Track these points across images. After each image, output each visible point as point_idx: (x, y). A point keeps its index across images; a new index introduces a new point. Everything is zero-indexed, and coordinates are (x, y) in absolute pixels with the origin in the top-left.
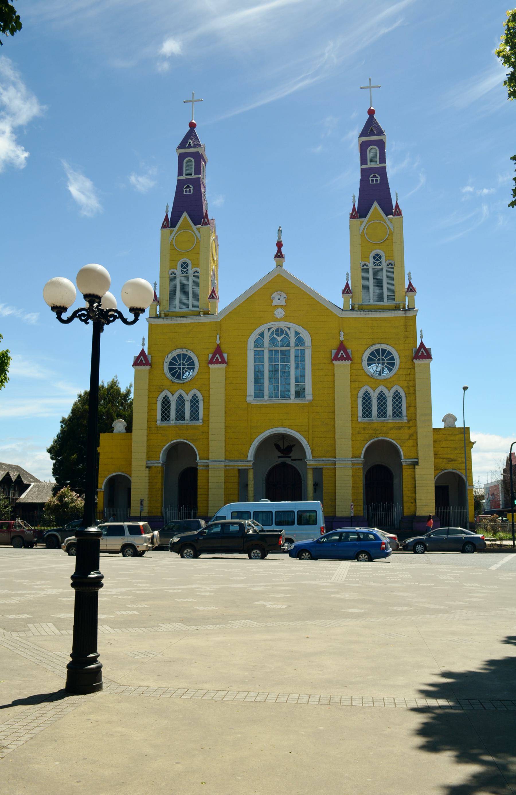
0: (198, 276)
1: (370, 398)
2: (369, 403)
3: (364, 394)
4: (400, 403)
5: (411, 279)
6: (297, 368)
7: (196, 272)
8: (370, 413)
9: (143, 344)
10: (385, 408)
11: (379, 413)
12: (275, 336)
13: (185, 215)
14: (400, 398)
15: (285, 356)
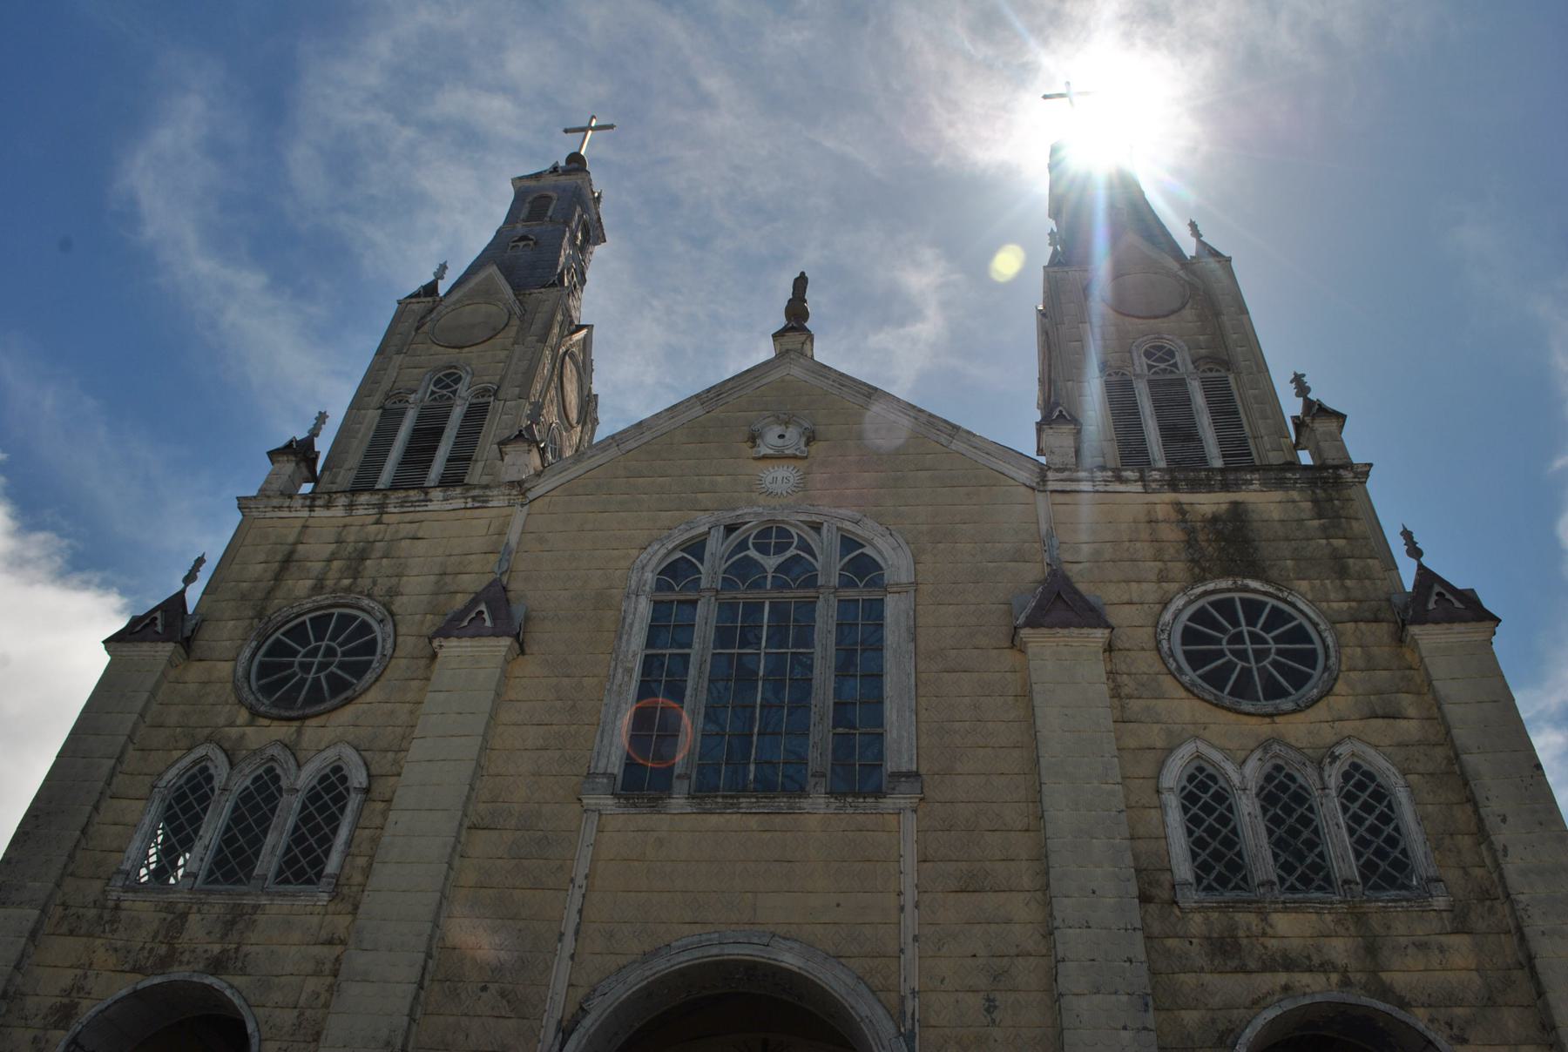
1: (1220, 797)
2: (1224, 820)
3: (1191, 778)
4: (1386, 819)
5: (1308, 390)
6: (844, 669)
8: (1236, 866)
9: (190, 578)
10: (1311, 845)
11: (1287, 868)
12: (753, 553)
14: (1380, 795)
15: (793, 624)
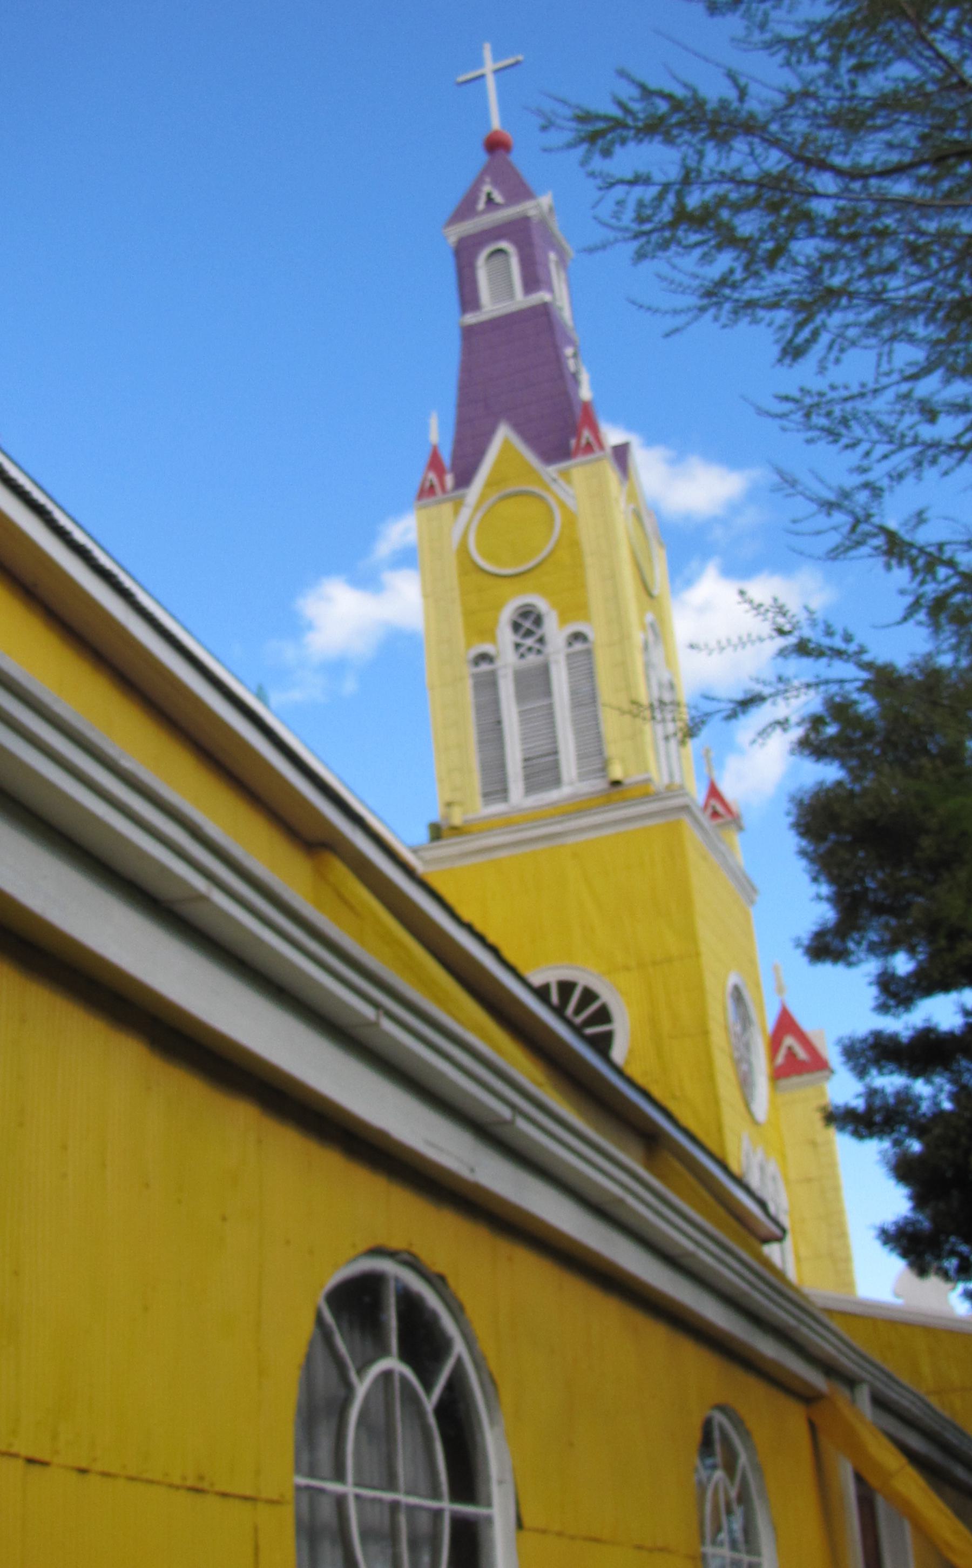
0: (589, 653)
7: (578, 636)
13: (503, 435)
